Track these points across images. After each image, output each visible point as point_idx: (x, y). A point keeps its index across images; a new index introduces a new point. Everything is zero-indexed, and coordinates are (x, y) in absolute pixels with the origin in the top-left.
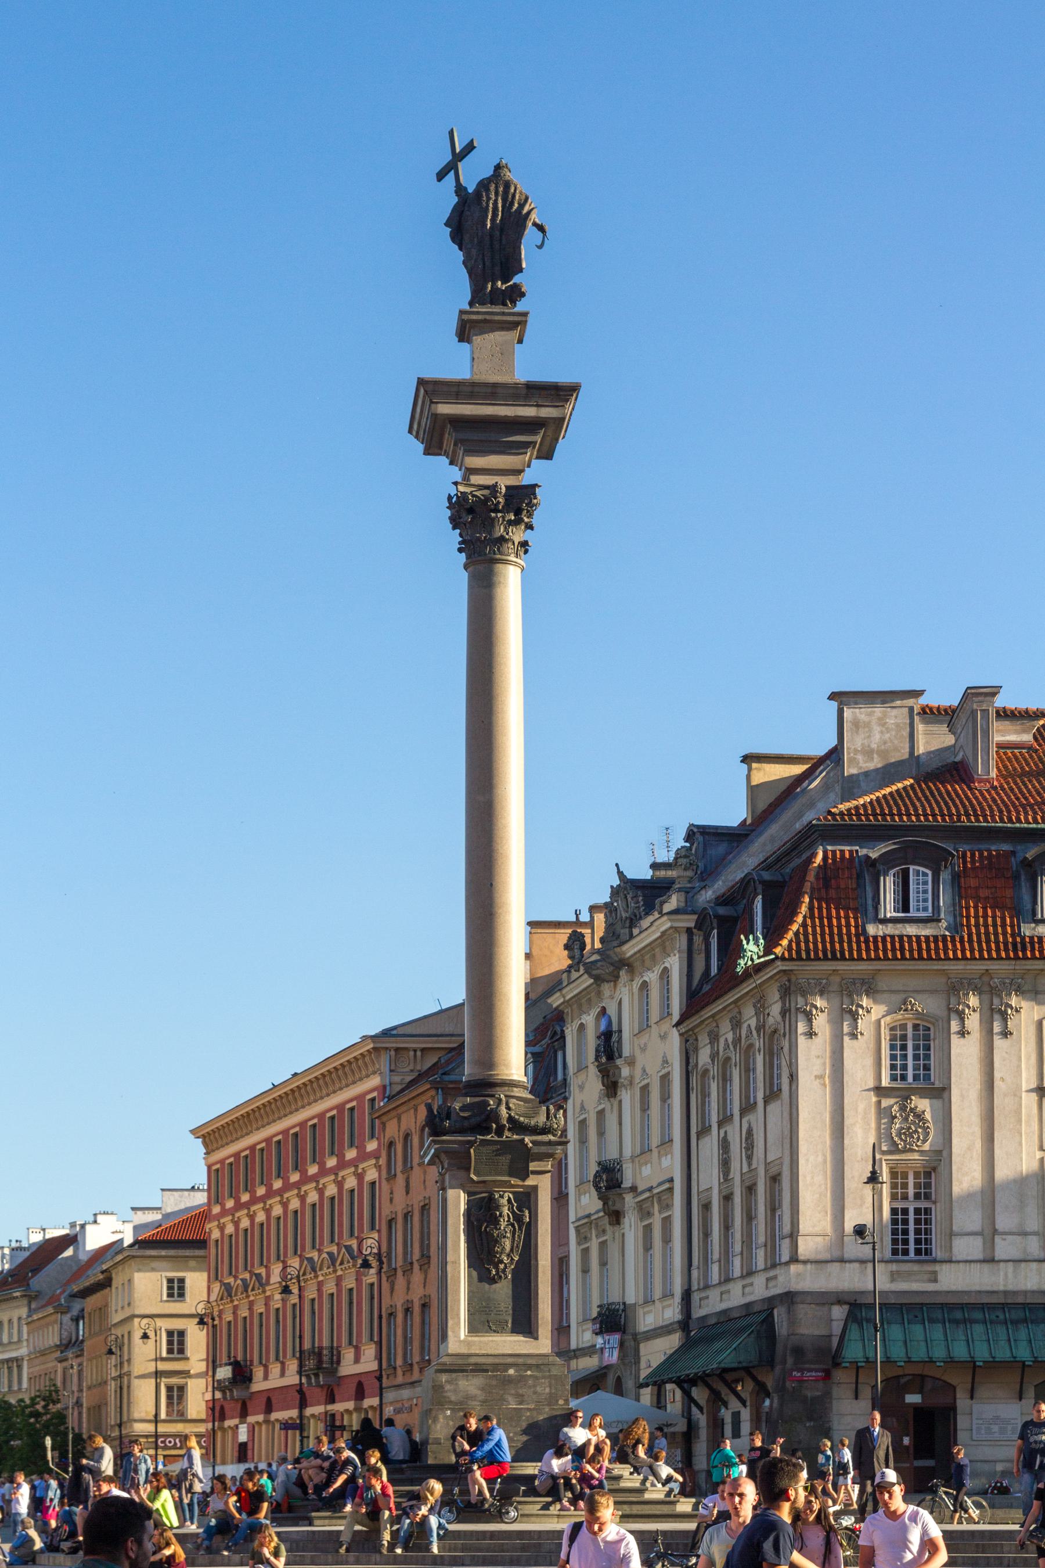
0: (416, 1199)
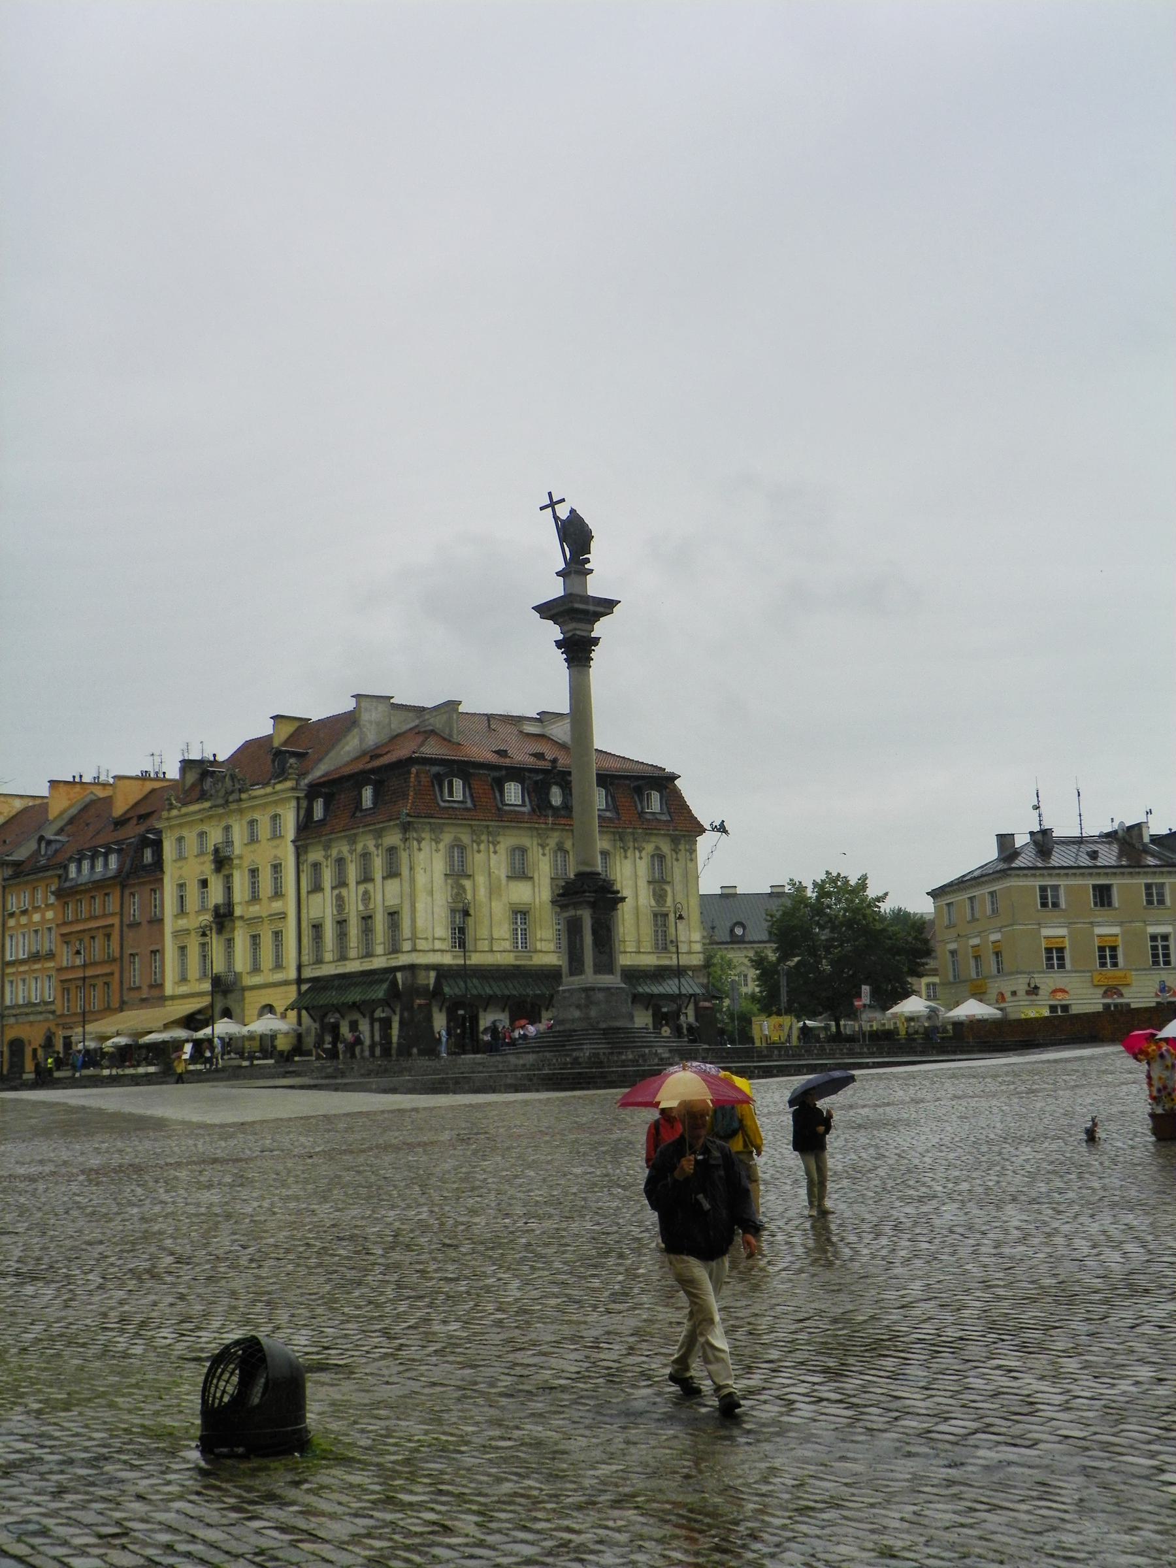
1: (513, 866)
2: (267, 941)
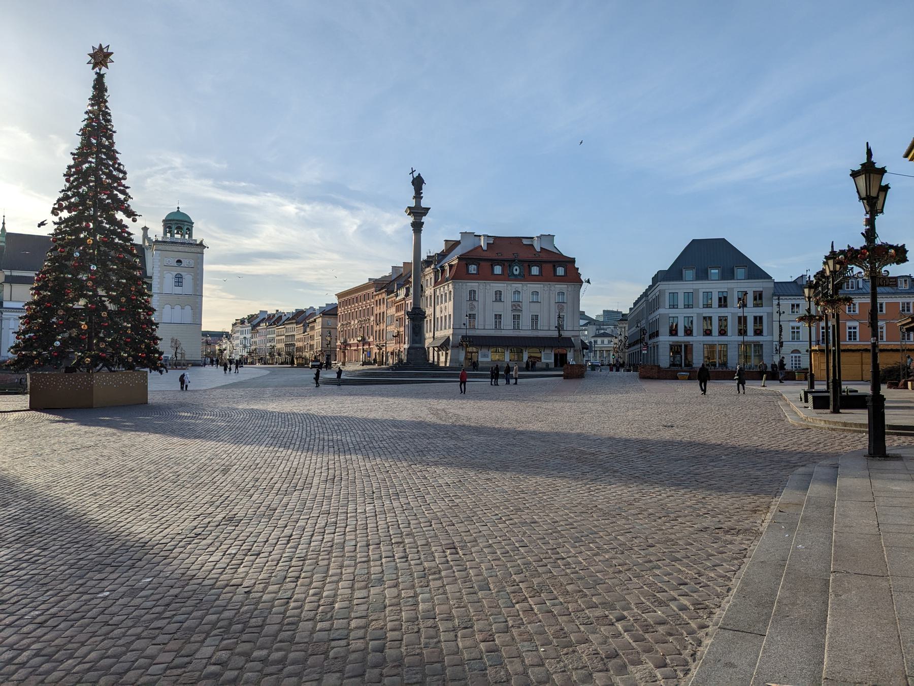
0: (382, 311)
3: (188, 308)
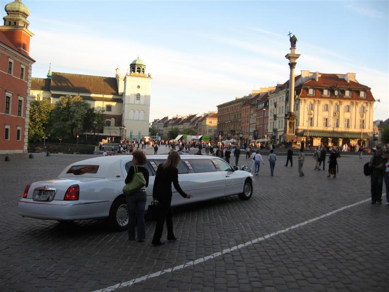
1: (325, 109)
2: (281, 122)
3: (142, 112)
